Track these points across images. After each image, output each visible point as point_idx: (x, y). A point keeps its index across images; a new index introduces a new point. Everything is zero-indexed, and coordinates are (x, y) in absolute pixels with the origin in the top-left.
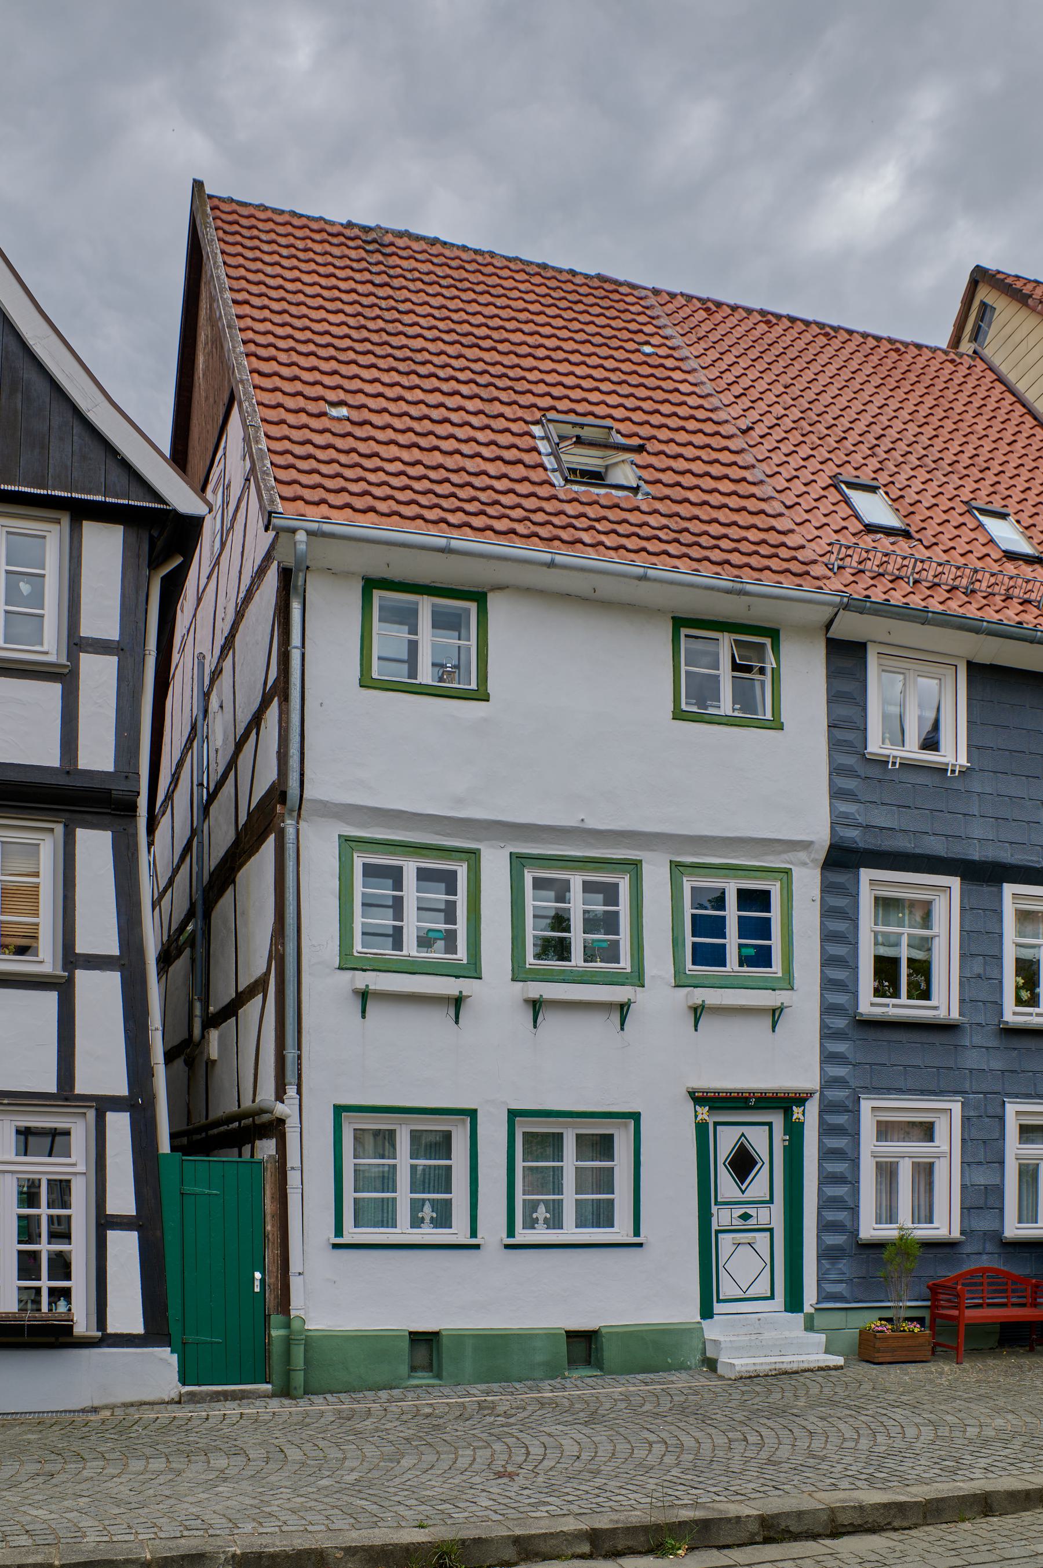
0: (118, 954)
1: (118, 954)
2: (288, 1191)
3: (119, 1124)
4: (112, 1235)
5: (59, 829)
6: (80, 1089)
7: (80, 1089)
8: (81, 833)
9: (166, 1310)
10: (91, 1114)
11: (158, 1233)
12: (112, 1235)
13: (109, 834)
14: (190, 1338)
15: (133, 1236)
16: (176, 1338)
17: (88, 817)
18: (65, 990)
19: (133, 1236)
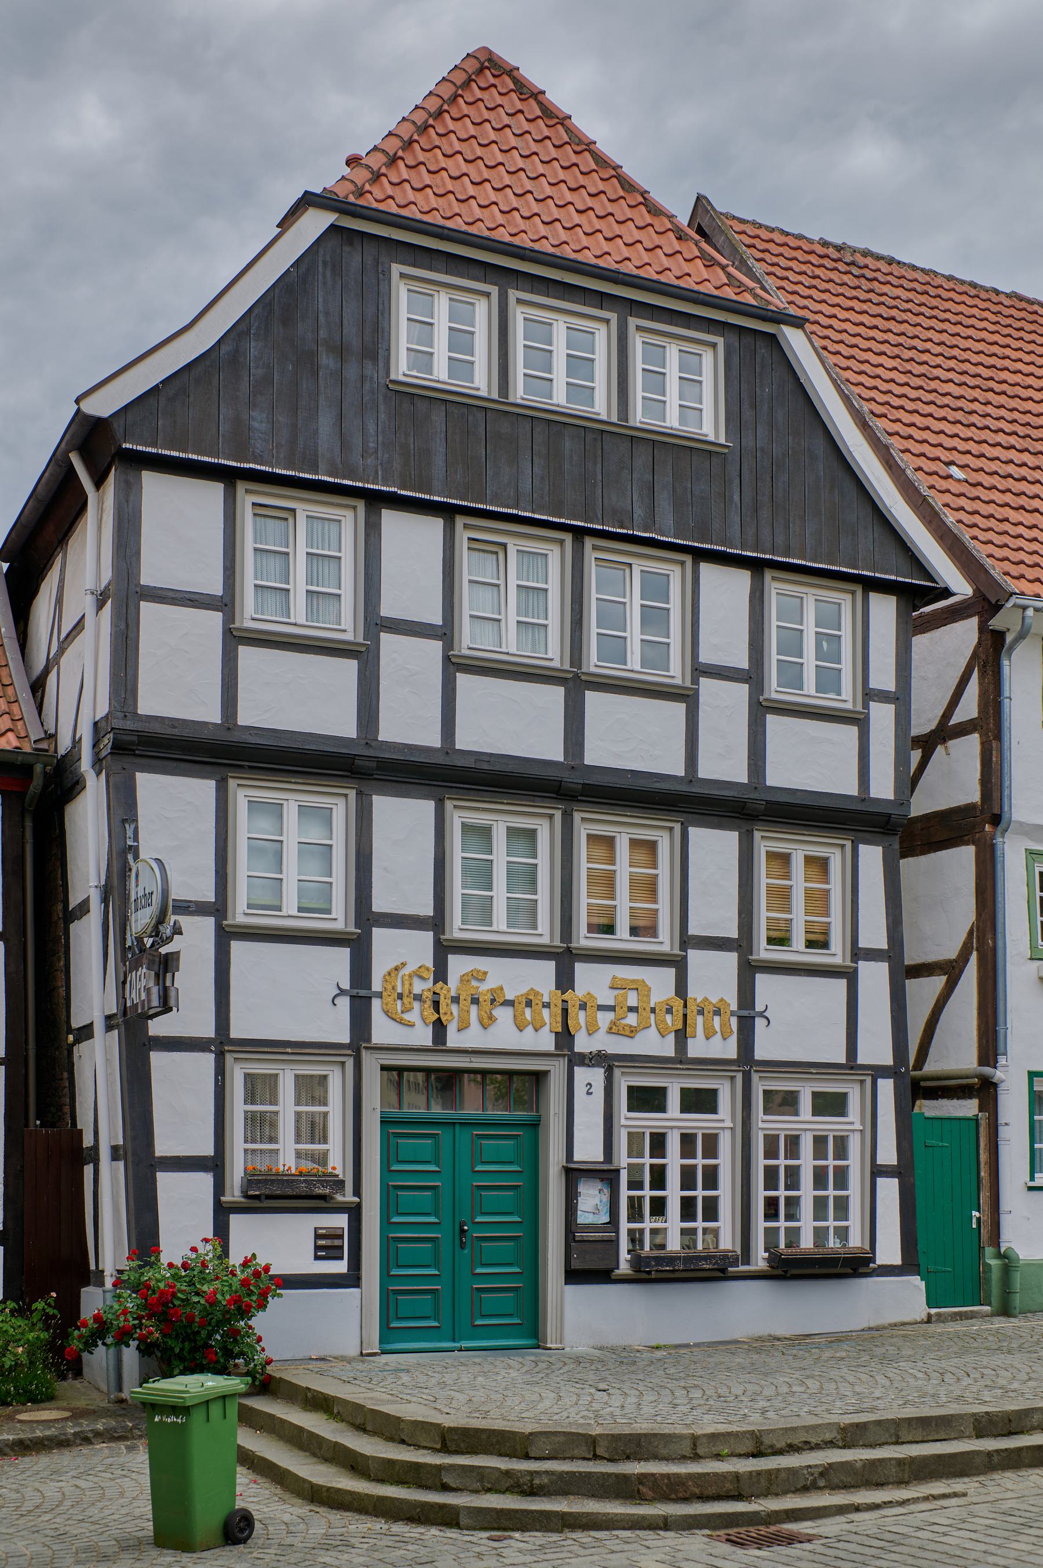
0: (886, 947)
1: (886, 947)
2: (999, 1143)
3: (886, 1087)
4: (880, 1181)
5: (848, 844)
6: (860, 1061)
7: (860, 1061)
8: (863, 848)
9: (917, 1245)
10: (869, 1080)
11: (912, 1180)
12: (880, 1181)
13: (880, 848)
14: (932, 1268)
15: (895, 1182)
16: (923, 1269)
17: (867, 835)
18: (851, 977)
19: (895, 1182)
